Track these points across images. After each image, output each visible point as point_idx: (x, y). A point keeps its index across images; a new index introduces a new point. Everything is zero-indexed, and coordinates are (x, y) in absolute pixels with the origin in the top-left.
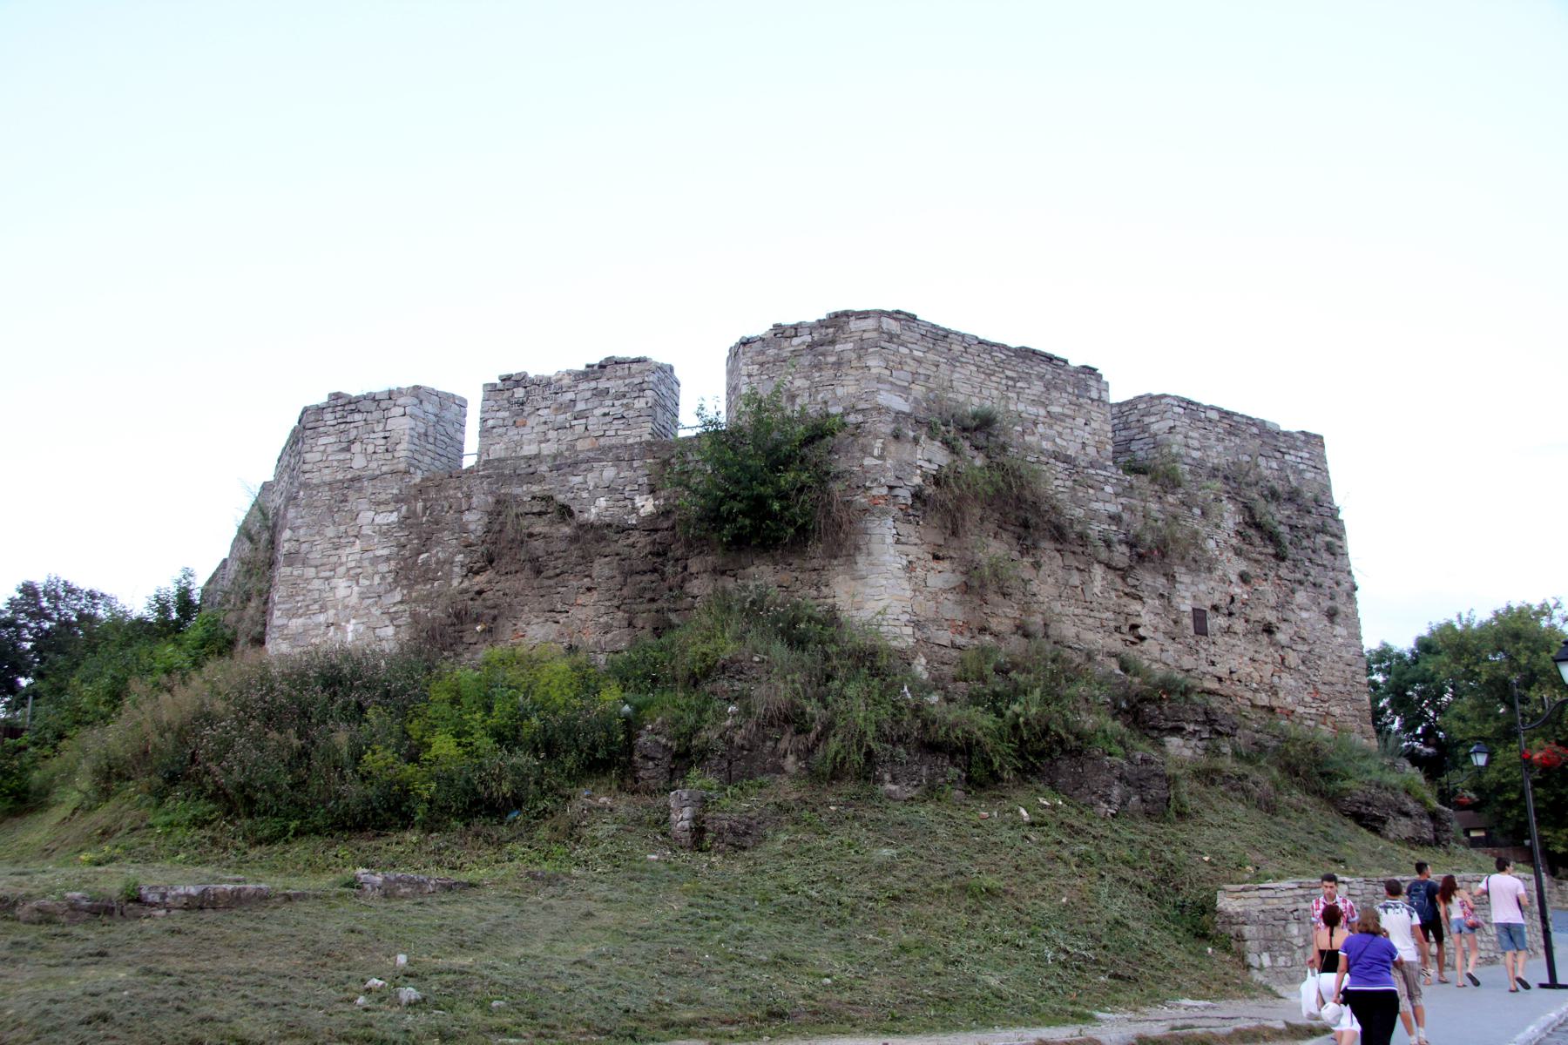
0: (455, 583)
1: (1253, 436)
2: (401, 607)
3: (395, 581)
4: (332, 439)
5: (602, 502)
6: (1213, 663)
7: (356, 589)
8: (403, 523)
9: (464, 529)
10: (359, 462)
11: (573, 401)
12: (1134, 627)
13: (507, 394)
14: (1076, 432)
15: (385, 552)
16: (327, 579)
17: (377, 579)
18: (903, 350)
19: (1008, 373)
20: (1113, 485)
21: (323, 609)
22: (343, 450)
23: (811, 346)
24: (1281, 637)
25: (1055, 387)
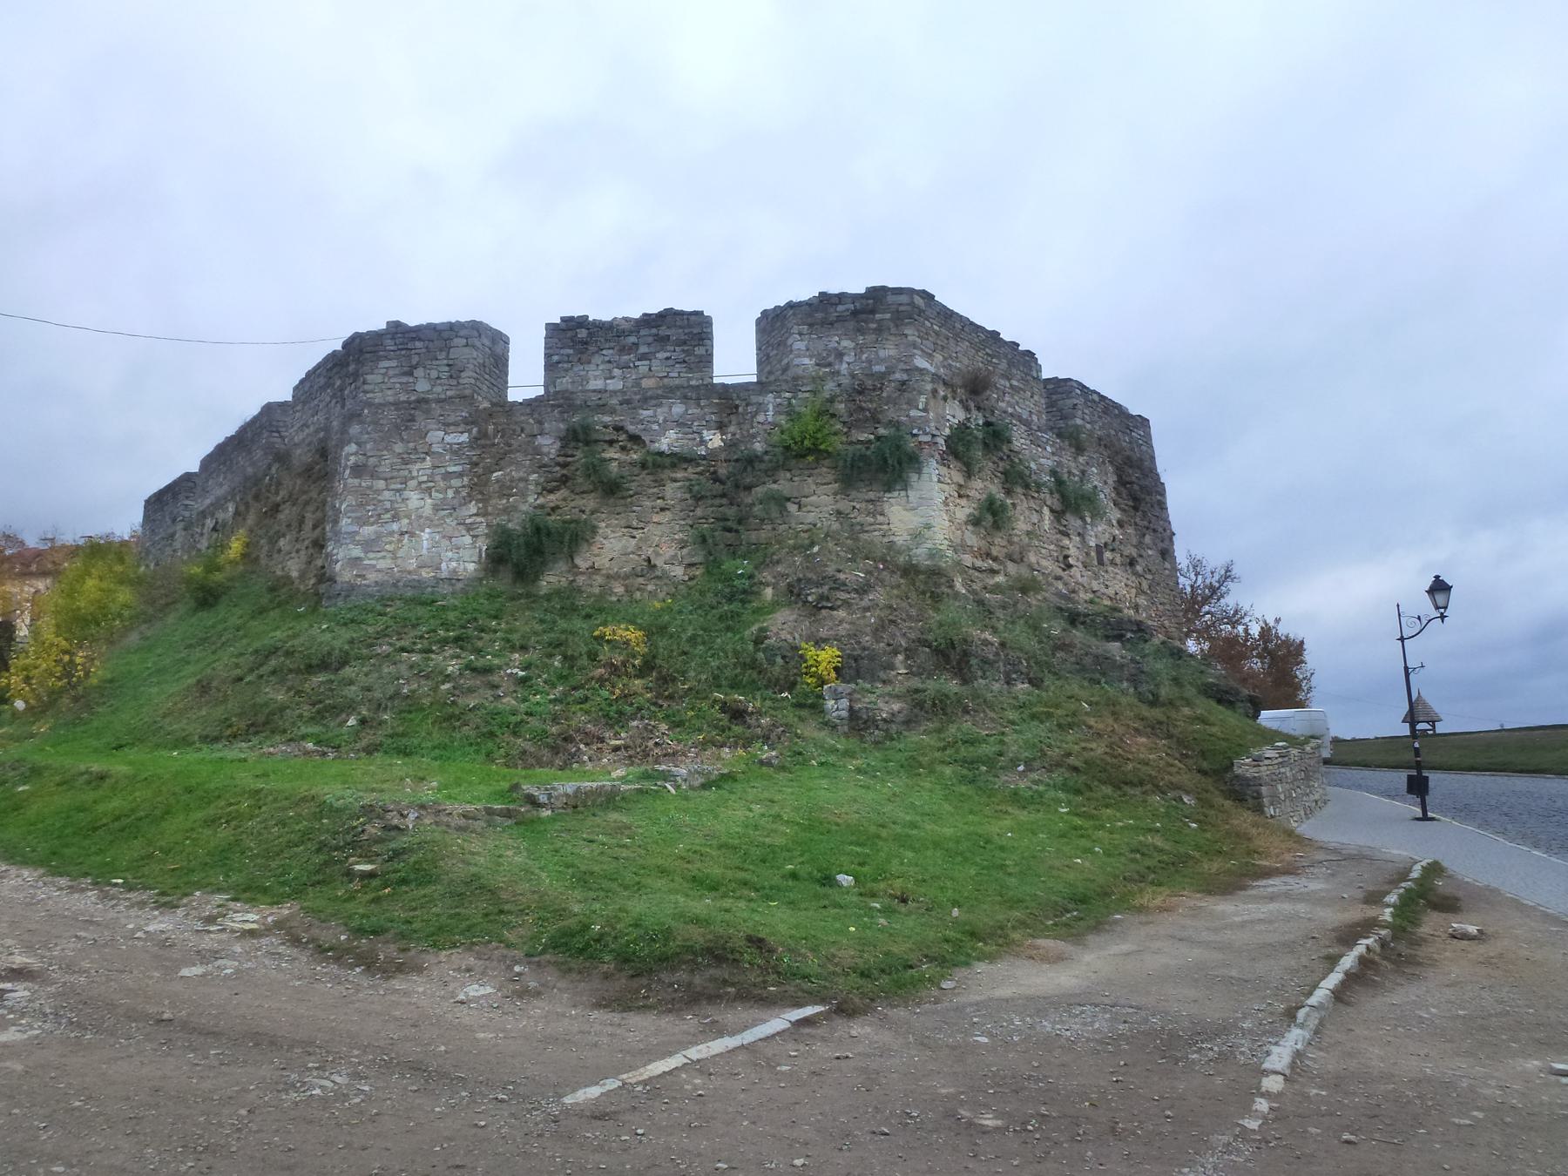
0: (531, 499)
2: (479, 519)
3: (469, 495)
4: (394, 363)
5: (672, 434)
7: (429, 501)
8: (474, 443)
9: (538, 451)
10: (422, 386)
11: (636, 345)
12: (1066, 557)
13: (570, 334)
15: (458, 469)
16: (398, 490)
17: (450, 494)
21: (396, 518)
22: (405, 374)
23: (855, 313)
24: (1139, 568)
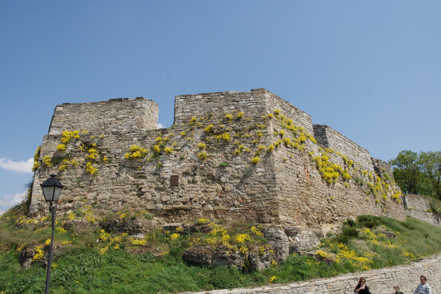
1: (221, 99)
6: (181, 197)
14: (128, 122)
18: (62, 115)
19: (101, 110)
20: (138, 137)
25: (121, 109)
